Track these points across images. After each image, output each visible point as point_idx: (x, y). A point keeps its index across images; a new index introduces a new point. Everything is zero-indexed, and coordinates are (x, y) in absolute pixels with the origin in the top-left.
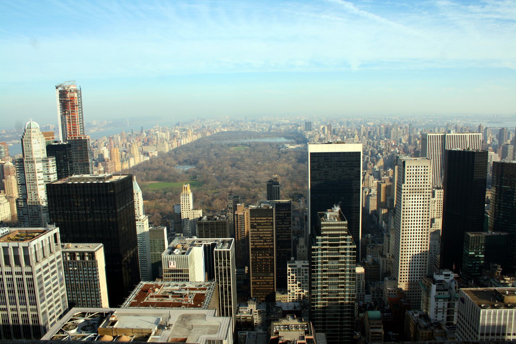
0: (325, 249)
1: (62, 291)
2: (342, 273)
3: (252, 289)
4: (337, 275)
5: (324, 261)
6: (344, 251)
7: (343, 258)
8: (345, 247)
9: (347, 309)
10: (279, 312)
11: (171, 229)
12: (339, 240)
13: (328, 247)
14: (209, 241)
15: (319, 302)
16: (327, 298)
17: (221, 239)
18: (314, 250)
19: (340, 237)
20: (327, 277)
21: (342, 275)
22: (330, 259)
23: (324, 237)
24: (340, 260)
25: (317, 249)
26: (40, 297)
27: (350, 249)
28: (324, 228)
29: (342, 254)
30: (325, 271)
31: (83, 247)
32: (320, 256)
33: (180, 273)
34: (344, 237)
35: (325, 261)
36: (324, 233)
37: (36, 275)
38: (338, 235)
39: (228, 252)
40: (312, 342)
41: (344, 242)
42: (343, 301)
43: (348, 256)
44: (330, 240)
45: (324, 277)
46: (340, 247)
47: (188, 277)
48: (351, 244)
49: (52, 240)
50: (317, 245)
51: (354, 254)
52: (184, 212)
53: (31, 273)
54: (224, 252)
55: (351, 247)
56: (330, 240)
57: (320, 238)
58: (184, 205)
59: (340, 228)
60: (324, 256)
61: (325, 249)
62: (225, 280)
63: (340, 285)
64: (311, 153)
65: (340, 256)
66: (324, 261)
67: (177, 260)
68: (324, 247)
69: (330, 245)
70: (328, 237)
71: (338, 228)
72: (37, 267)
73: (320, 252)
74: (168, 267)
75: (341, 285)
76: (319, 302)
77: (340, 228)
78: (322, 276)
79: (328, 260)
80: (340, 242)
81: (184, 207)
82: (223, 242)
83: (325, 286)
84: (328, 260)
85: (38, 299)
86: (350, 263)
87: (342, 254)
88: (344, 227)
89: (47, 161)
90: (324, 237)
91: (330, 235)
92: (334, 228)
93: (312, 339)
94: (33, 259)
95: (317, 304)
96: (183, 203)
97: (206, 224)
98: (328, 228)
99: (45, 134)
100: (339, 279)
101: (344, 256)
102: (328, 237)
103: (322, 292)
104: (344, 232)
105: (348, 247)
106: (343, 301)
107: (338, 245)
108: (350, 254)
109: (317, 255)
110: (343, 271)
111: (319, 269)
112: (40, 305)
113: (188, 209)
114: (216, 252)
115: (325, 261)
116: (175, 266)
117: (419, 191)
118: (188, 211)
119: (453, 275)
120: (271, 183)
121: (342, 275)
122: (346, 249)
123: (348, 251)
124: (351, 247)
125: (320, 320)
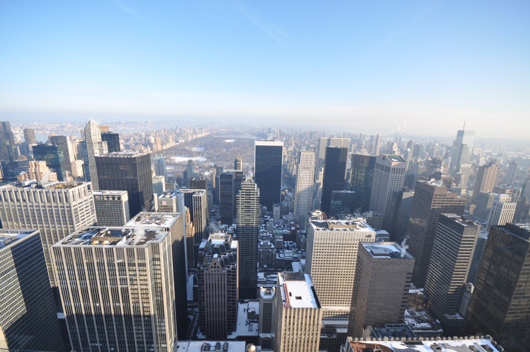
1: (93, 217)
12: (250, 193)
14: (191, 191)
22: (246, 202)
26: (76, 220)
31: (115, 192)
37: (73, 208)
38: (250, 190)
39: (200, 197)
49: (86, 188)
53: (70, 207)
67: (167, 200)
69: (246, 195)
72: (73, 203)
82: (199, 192)
85: (75, 222)
89: (101, 143)
91: (246, 190)
94: (71, 199)
99: (100, 127)
105: (255, 196)
107: (250, 195)
112: (76, 225)
117: (308, 168)
119: (321, 213)
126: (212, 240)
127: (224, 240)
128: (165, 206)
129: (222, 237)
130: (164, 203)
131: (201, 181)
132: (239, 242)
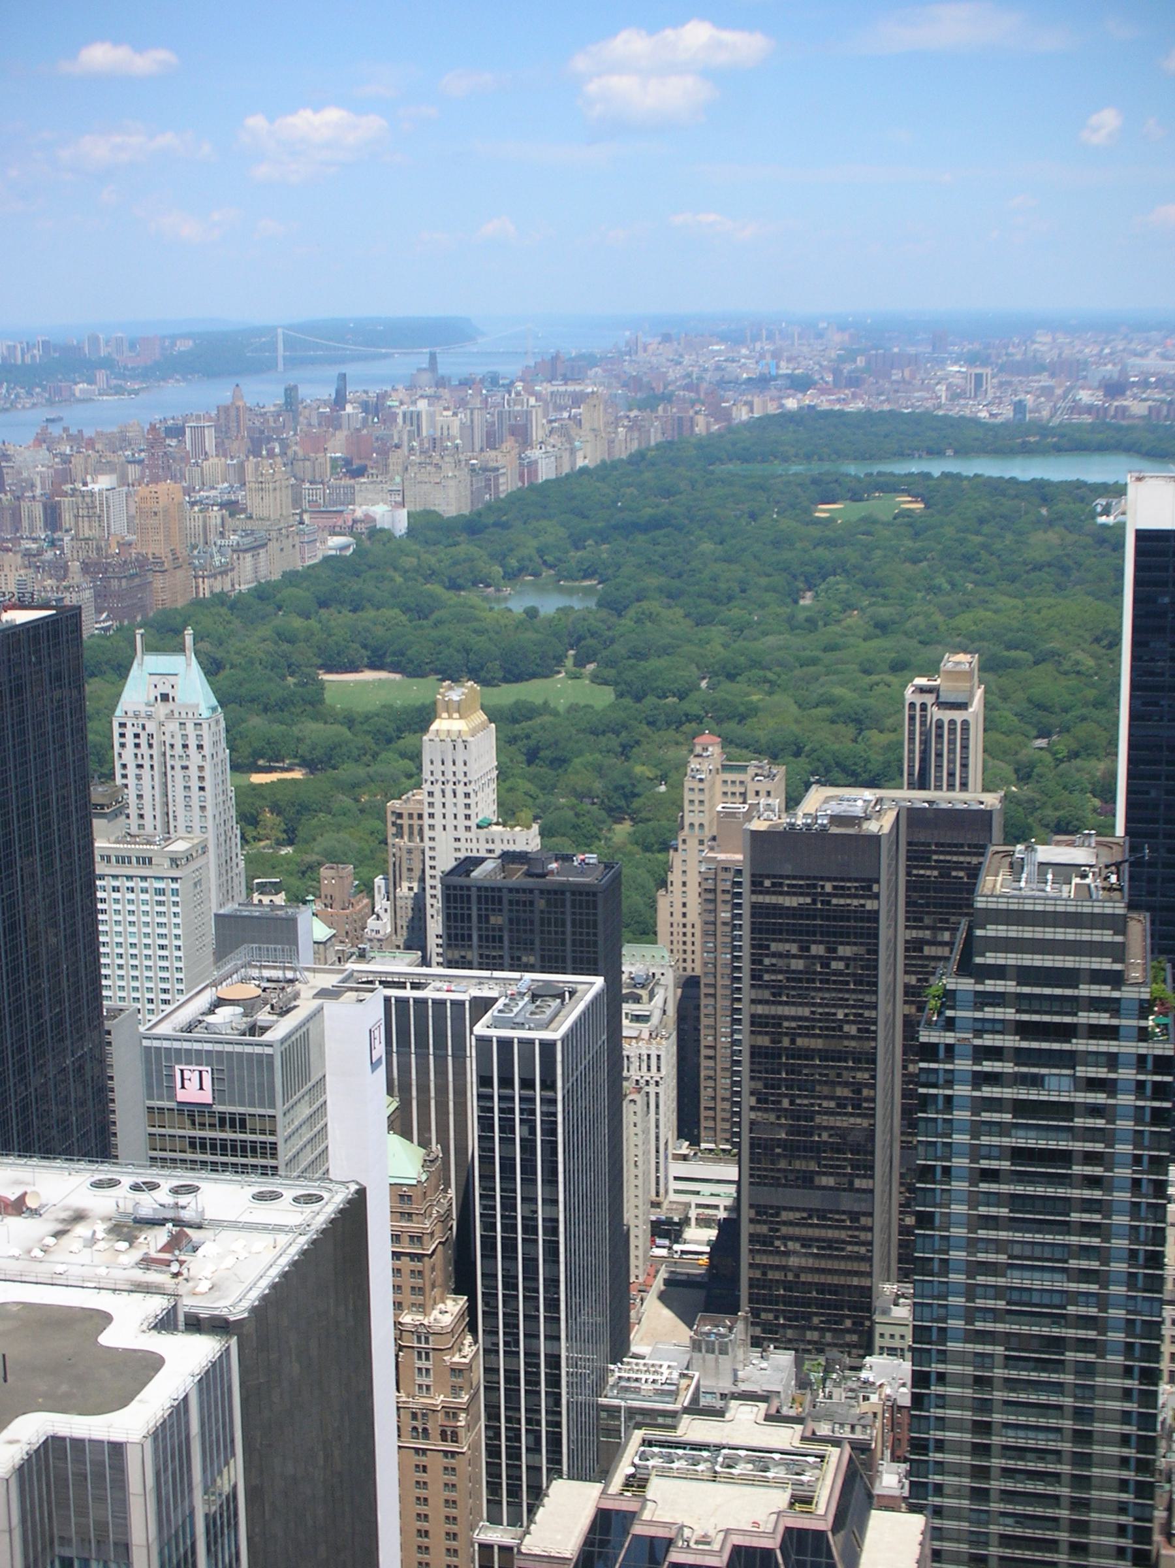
0: (995, 1053)
2: (1087, 1194)
3: (745, 1274)
4: (1067, 1204)
5: (986, 1116)
6: (1102, 1073)
7: (1095, 1111)
8: (1111, 1046)
9: (1116, 1405)
10: (865, 1407)
11: (371, 922)
12: (1074, 1004)
13: (1011, 1041)
15: (952, 1346)
16: (1000, 1327)
17: (528, 976)
18: (929, 1052)
19: (1084, 990)
20: (1004, 1212)
21: (1089, 1206)
22: (1020, 1108)
23: (990, 985)
24: (1079, 1122)
25: (950, 1048)
27: (1142, 1059)
28: (991, 931)
29: (1093, 1084)
30: (991, 1175)
32: (962, 1090)
33: (228, 1135)
34: (1105, 991)
35: (996, 1117)
36: (991, 959)
38: (1070, 977)
39: (548, 1047)
40: (817, 1552)
41: (1104, 1019)
42: (1091, 1357)
43: (1126, 1100)
44: (1020, 1002)
45: (983, 1210)
46: (1079, 1045)
47: (274, 1155)
48: (1144, 1035)
50: (950, 1025)
51: (1160, 1091)
52: (438, 833)
54: (527, 1043)
55: (1143, 1048)
56: (1020, 1002)
57: (966, 985)
58: (438, 799)
59: (1085, 935)
60: (988, 1091)
61: (995, 1053)
62: (529, 1200)
63: (1073, 1263)
64: (1141, 535)
65: (1081, 1097)
66: (986, 1116)
68: (988, 1040)
69: (1024, 1029)
70: (1009, 986)
71: (1070, 934)
73: (963, 1065)
74: (172, 1096)
75: (1084, 1264)
76: (952, 1346)
77: (1085, 935)
78: (973, 1200)
79: (1007, 1117)
80: (1085, 1018)
81: (438, 810)
83: (992, 1257)
84: (1007, 1117)
86: (1137, 1138)
87: (1093, 1084)
88: (1107, 936)
90: (990, 985)
91: (1025, 975)
92: (1049, 933)
93: (820, 1535)
95: (943, 1357)
96: (437, 789)
97: (491, 896)
98: (1013, 932)
100: (1066, 1228)
101: (1100, 1098)
102: (1009, 986)
103: (970, 1292)
104: (1106, 964)
105: (1128, 1047)
106: (1091, 1357)
107: (1067, 1032)
108: (1141, 1085)
109: (949, 1084)
110: (1093, 1182)
111: (960, 1162)
113: (462, 822)
114: (484, 1041)
115: (996, 1117)
116: (206, 1097)
118: (462, 833)
120: (929, 699)
121: (1089, 1206)
122: (1112, 1060)
123: (1127, 1074)
124: (1143, 1048)
125: (958, 1448)
126: (656, 1488)
127: (780, 1498)
128: (193, 1113)
129: (761, 1457)
130: (195, 1087)
131: (556, 894)
132: (934, 1533)
